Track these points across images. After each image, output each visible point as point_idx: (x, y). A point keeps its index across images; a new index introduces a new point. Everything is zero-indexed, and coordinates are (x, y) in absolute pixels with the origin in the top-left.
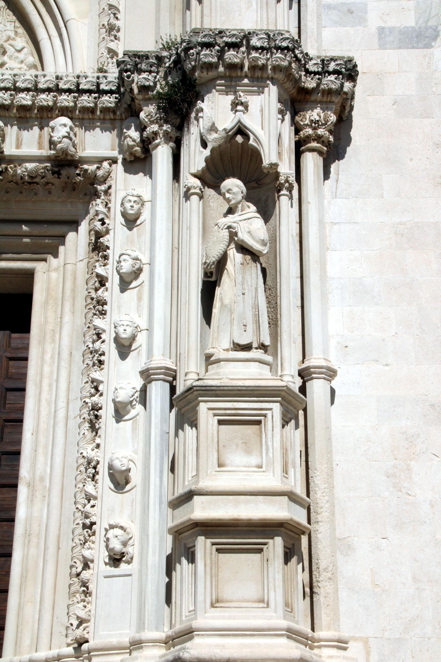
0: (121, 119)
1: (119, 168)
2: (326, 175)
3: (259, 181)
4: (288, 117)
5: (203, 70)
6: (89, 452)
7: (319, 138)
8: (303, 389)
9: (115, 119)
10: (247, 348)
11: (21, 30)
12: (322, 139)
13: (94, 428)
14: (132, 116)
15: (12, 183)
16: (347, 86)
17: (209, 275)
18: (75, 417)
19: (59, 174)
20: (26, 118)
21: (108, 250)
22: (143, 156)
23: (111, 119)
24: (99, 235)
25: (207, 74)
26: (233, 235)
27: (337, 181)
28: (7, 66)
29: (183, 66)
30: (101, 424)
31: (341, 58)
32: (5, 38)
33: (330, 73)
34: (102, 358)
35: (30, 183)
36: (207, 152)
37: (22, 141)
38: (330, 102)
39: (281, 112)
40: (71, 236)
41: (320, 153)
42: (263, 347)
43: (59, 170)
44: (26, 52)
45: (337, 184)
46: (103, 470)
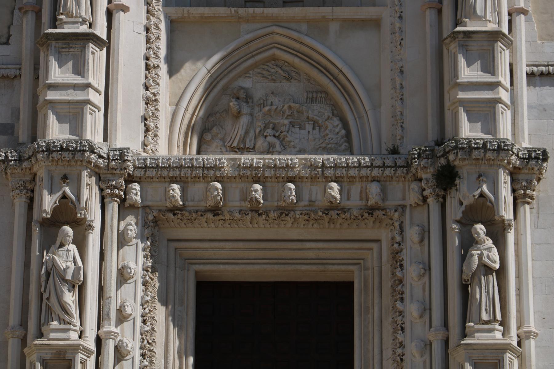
0: (409, 181)
3: (493, 221)
5: (460, 161)
9: (405, 181)
12: (529, 195)
14: (416, 180)
15: (344, 219)
17: (466, 280)
18: (388, 359)
19: (372, 214)
20: (353, 181)
21: (403, 261)
22: (423, 204)
23: (402, 181)
25: (463, 163)
27: (538, 217)
28: (329, 136)
29: (448, 157)
31: (539, 150)
32: (326, 117)
33: (533, 159)
34: (403, 326)
35: (354, 219)
36: (463, 208)
37: (350, 195)
38: (533, 173)
43: (373, 212)
44: (341, 127)
45: (538, 219)
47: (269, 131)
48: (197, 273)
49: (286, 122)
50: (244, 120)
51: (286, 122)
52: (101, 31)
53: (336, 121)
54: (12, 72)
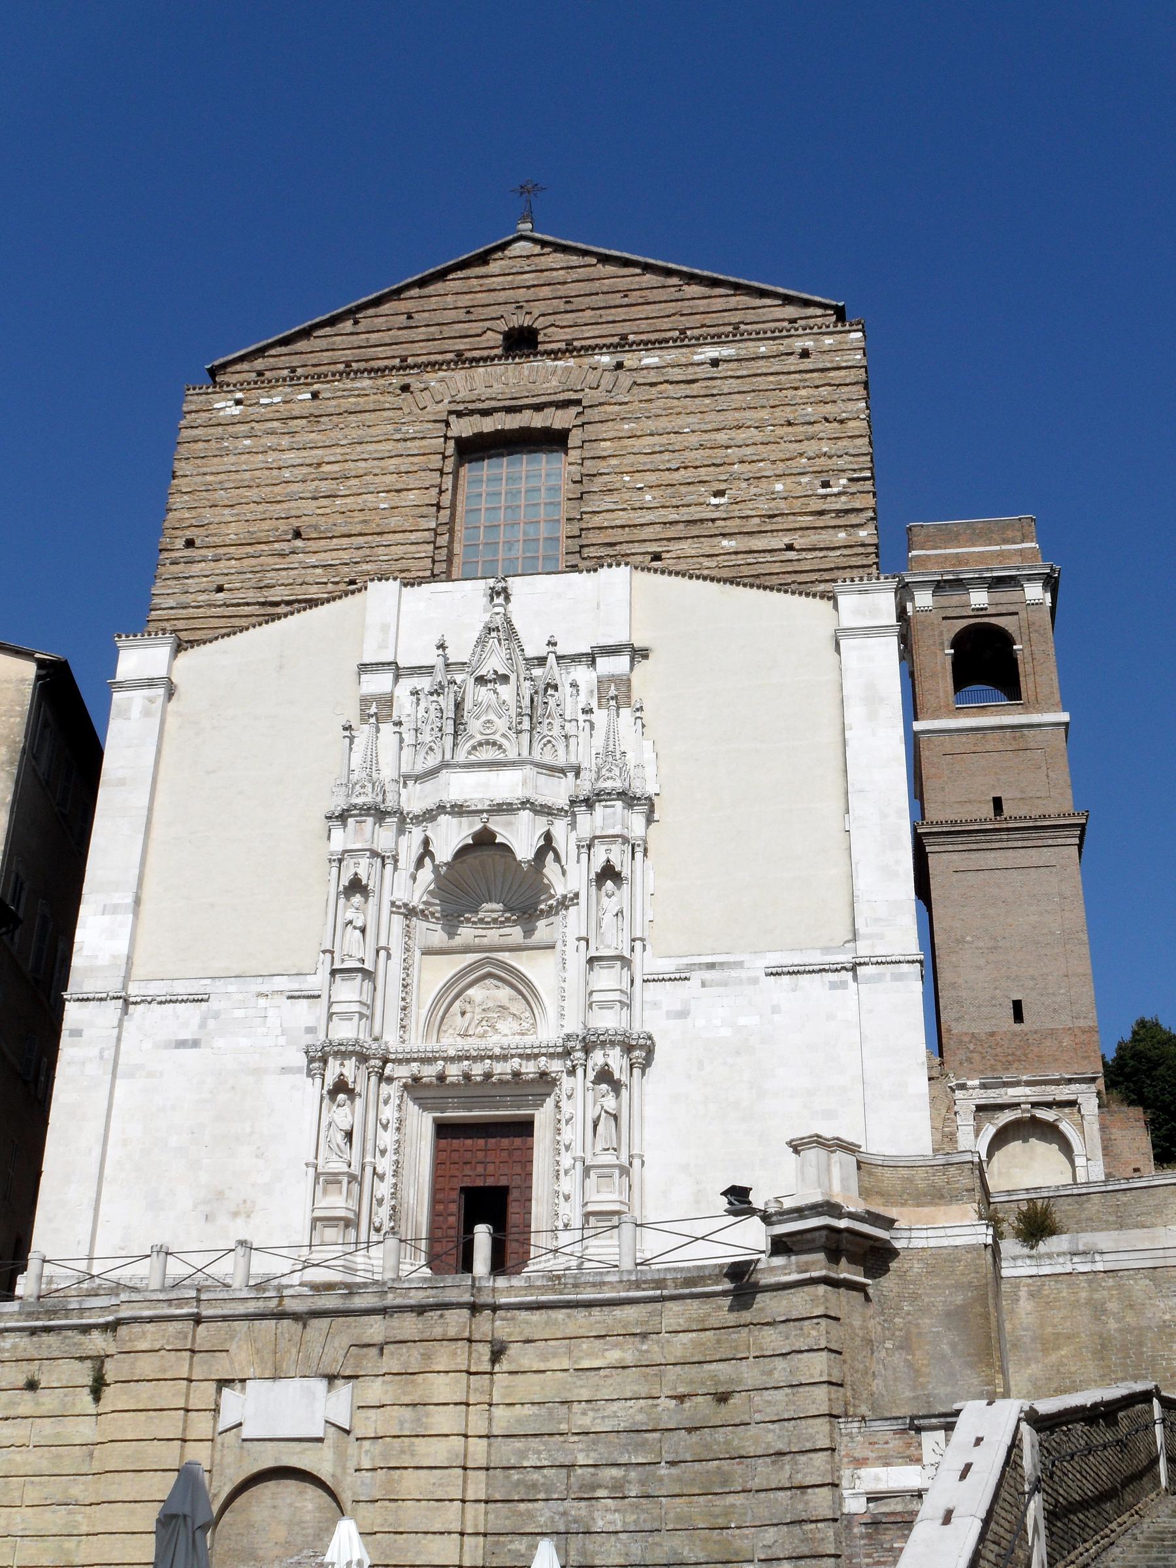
1: (565, 1074)
2: (643, 1074)
4: (625, 1056)
6: (556, 1188)
7: (639, 1063)
8: (631, 1164)
10: (608, 1149)
11: (528, 1008)
13: (558, 1179)
16: (649, 1042)
24: (558, 1102)
26: (602, 1107)
30: (560, 1177)
39: (623, 1056)
40: (548, 1099)
42: (615, 1150)
46: (561, 1194)
47: (484, 1023)
48: (435, 1119)
49: (496, 1016)
50: (468, 1016)
51: (496, 1016)
52: (368, 966)
53: (527, 1014)
54: (316, 993)
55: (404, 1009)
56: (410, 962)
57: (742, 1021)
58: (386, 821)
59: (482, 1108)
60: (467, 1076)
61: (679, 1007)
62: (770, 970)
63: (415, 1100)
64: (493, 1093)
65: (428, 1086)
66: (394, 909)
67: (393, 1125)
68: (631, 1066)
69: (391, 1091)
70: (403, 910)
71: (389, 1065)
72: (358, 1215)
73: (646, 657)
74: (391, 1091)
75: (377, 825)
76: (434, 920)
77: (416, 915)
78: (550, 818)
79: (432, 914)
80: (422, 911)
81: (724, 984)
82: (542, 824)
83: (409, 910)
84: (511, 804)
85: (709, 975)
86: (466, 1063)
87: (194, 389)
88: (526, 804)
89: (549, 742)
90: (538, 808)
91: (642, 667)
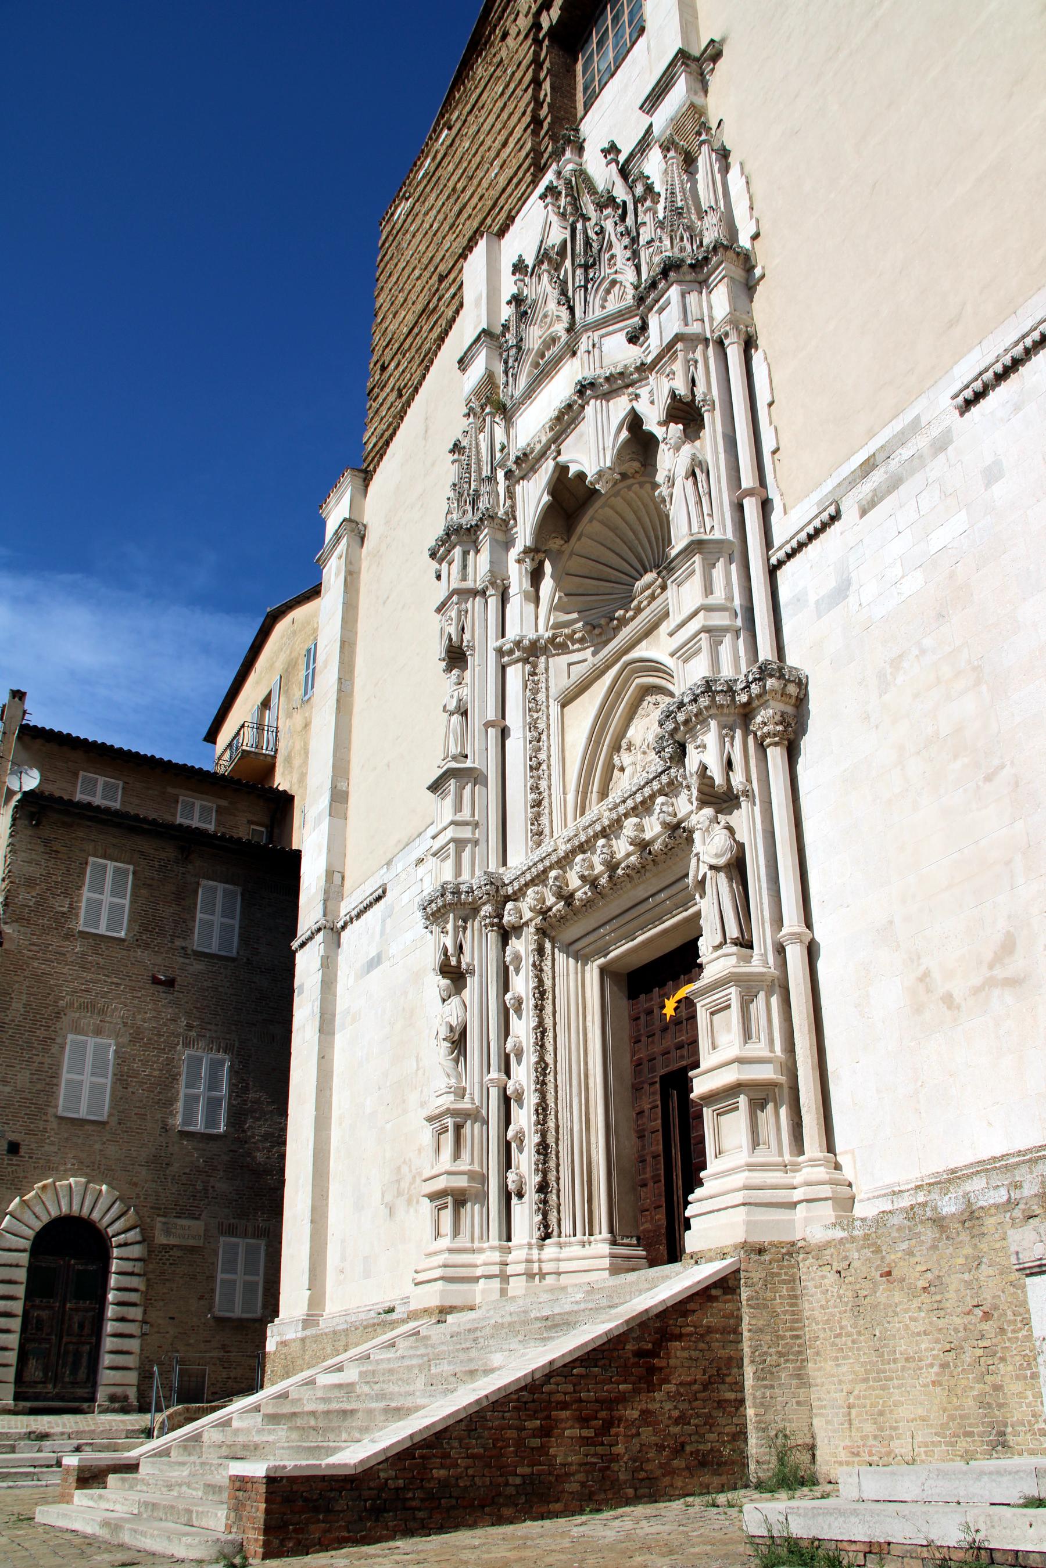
41: (776, 744)
48: (603, 971)
55: (538, 804)
56: (541, 725)
57: (938, 539)
58: (481, 537)
59: (643, 928)
60: (592, 882)
61: (832, 583)
62: (960, 400)
63: (568, 948)
64: (641, 893)
65: (562, 919)
66: (506, 659)
67: (529, 1004)
68: (762, 748)
69: (522, 946)
70: (517, 654)
71: (509, 905)
72: (484, 1179)
73: (716, 57)
74: (522, 946)
75: (472, 553)
76: (577, 646)
77: (545, 650)
78: (631, 390)
79: (570, 637)
80: (552, 640)
81: (894, 483)
82: (620, 407)
83: (524, 650)
84: (569, 406)
85: (865, 489)
86: (579, 858)
87: (384, 219)
88: (584, 389)
89: (614, 283)
90: (606, 387)
91: (720, 76)
